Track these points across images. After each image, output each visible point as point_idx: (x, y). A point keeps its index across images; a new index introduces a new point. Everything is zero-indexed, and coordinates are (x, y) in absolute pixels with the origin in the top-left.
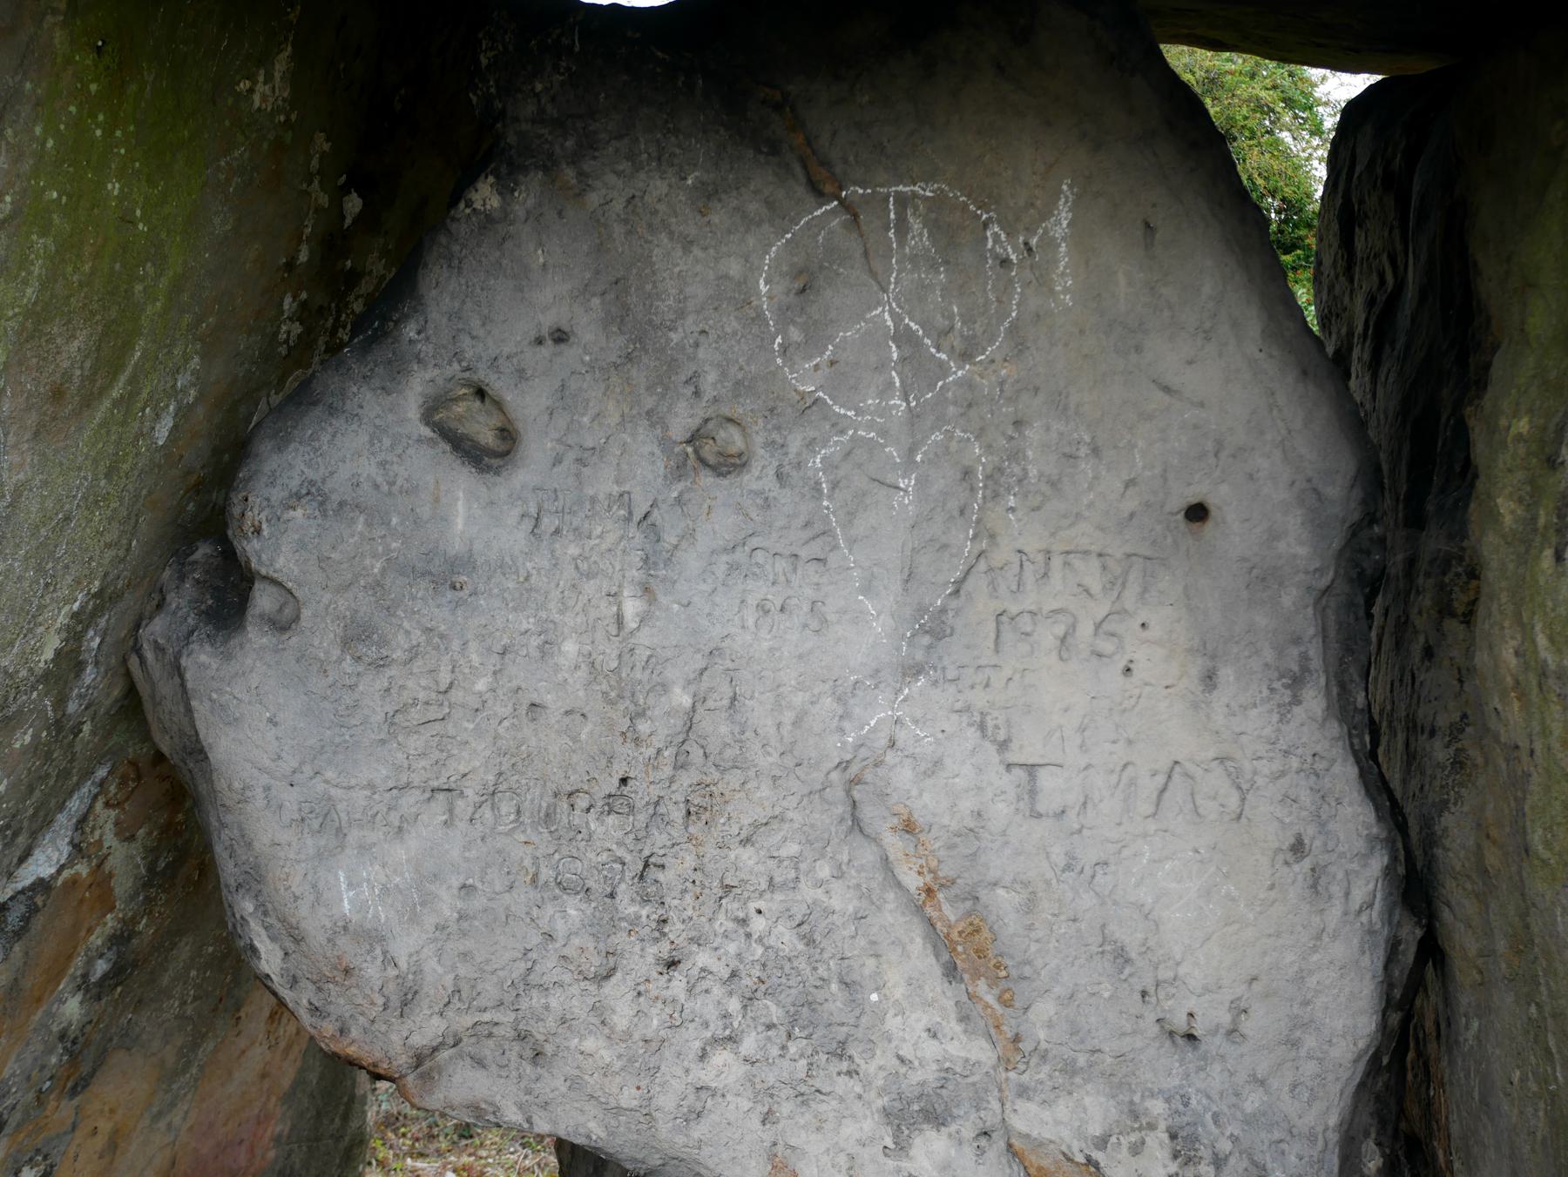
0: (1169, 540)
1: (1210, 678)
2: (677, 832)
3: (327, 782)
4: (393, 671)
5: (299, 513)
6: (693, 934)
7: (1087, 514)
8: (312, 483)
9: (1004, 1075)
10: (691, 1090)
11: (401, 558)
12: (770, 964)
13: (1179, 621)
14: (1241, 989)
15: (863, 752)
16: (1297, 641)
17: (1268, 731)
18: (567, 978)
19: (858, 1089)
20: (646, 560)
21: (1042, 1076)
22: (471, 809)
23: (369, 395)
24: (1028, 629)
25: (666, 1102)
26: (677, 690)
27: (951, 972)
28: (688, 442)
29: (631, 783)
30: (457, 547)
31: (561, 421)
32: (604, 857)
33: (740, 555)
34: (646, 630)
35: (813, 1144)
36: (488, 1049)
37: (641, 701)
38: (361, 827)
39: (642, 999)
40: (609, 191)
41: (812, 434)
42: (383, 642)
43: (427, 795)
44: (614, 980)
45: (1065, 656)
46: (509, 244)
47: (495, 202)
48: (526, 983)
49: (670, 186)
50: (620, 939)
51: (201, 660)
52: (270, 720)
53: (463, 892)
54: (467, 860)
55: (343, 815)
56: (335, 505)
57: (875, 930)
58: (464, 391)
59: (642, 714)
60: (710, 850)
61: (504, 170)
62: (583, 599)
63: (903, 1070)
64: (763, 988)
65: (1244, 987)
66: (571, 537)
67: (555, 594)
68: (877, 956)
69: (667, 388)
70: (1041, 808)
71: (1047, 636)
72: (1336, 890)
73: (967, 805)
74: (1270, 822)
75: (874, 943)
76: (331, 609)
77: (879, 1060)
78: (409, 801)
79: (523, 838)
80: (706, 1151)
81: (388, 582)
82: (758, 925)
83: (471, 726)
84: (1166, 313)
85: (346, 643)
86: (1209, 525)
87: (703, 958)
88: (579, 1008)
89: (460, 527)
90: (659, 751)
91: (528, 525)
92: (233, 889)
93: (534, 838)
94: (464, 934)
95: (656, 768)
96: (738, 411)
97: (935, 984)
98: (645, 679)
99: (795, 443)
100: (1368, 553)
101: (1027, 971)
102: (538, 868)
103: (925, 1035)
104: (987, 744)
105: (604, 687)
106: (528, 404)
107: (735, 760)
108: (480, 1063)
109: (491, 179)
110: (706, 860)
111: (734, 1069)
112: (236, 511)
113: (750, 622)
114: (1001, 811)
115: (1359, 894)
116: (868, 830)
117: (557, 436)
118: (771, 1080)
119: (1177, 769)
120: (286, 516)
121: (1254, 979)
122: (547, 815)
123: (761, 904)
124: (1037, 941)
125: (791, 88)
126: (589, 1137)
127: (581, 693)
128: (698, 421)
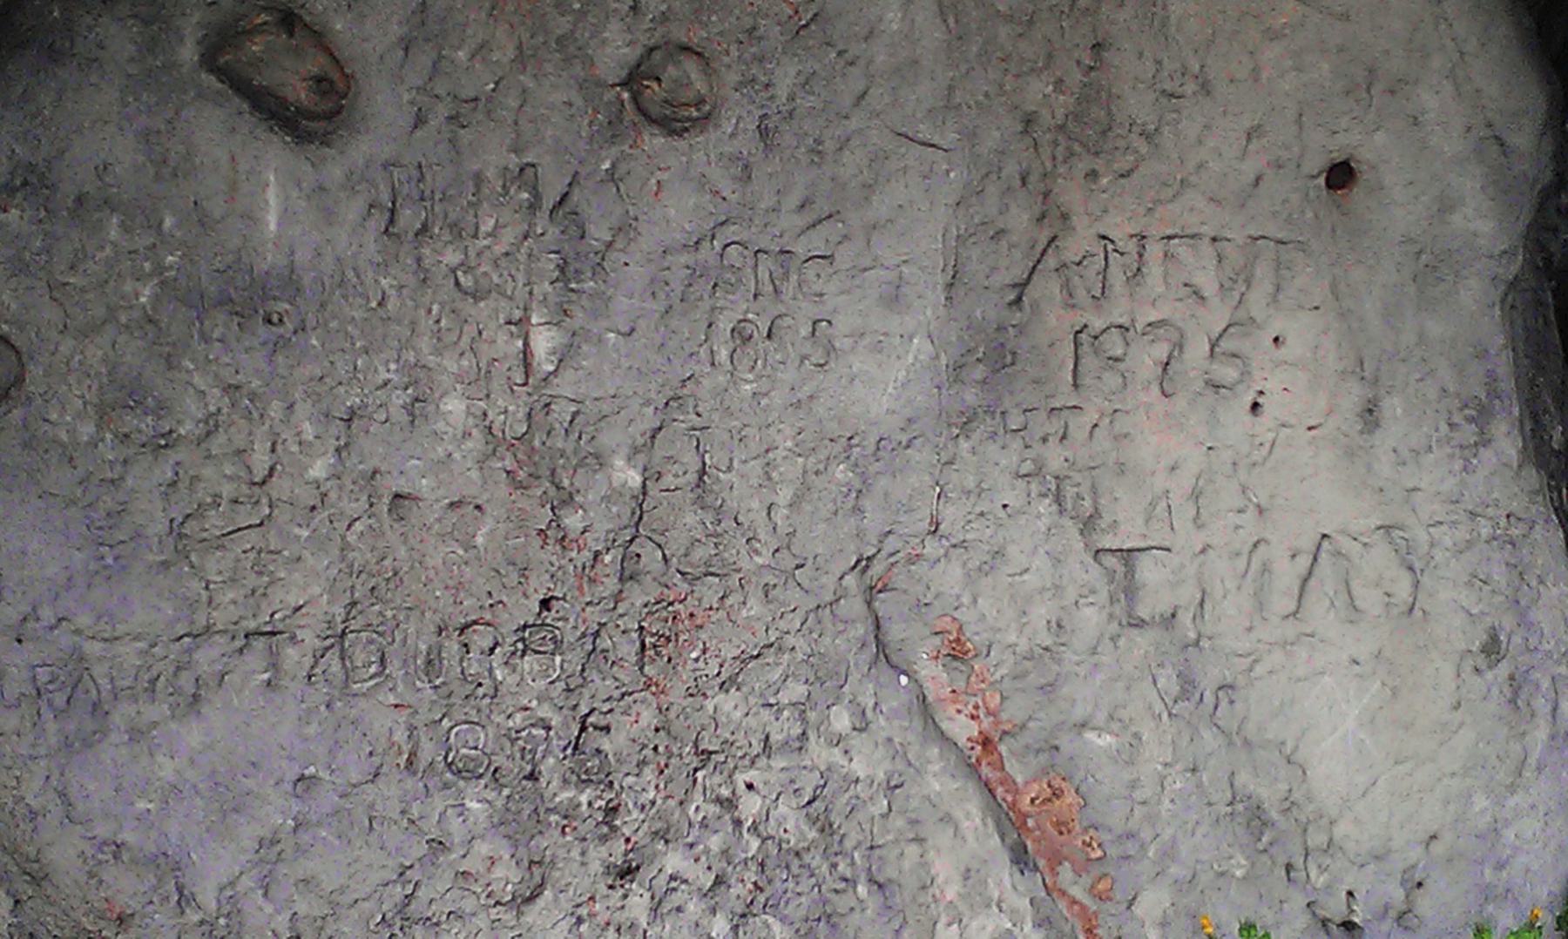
0: (1309, 215)
1: (1370, 411)
3: (78, 632)
4: (180, 454)
5: (14, 213)
6: (659, 825)
7: (1193, 179)
8: (31, 167)
11: (183, 282)
12: (770, 863)
14: (1416, 854)
16: (1482, 355)
17: (1450, 485)
18: (469, 905)
20: (562, 269)
22: (308, 661)
24: (1119, 352)
26: (619, 462)
27: (1020, 858)
28: (623, 84)
29: (555, 605)
30: (271, 259)
31: (423, 59)
33: (707, 253)
34: (568, 375)
37: (566, 483)
38: (135, 699)
39: (584, 928)
41: (811, 65)
42: (161, 410)
44: (540, 902)
50: (548, 842)
55: (104, 682)
56: (70, 203)
57: (914, 803)
59: (569, 500)
60: (676, 695)
62: (469, 330)
65: (1420, 850)
66: (447, 237)
67: (427, 324)
68: (919, 840)
70: (1143, 612)
71: (1146, 357)
72: (1542, 705)
73: (1041, 612)
75: (914, 822)
76: (75, 364)
78: (207, 658)
79: (392, 700)
82: (751, 807)
83: (305, 533)
85: (103, 416)
86: (1358, 193)
87: (674, 861)
89: (273, 227)
90: (597, 555)
91: (379, 220)
93: (409, 698)
95: (592, 581)
96: (696, 37)
97: (1002, 876)
98: (570, 447)
99: (784, 86)
101: (1131, 848)
102: (417, 744)
105: (509, 463)
107: (708, 564)
110: (672, 715)
113: (723, 355)
114: (1091, 619)
116: (894, 659)
119: (1326, 544)
121: (1434, 837)
122: (429, 662)
124: (1144, 803)
127: (474, 474)
128: (639, 51)
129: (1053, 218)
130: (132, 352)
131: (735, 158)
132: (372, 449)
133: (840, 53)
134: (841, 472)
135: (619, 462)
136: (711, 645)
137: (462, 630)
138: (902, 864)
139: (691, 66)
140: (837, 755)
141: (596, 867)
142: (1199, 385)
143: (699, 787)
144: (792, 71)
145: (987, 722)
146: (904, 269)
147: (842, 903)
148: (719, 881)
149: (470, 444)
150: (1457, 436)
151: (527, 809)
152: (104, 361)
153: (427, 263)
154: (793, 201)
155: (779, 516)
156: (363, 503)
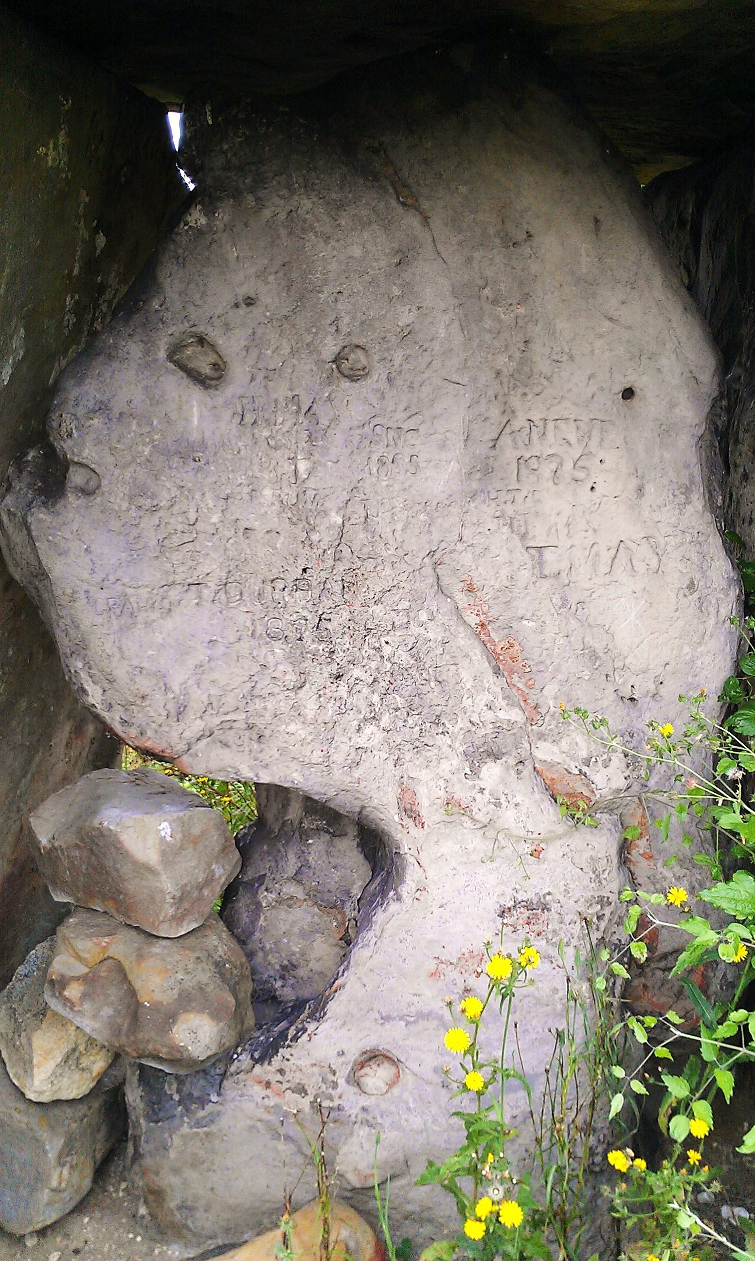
2: (337, 598)
3: (124, 585)
5: (96, 420)
8: (101, 402)
9: (530, 728)
10: (353, 749)
11: (161, 445)
13: (622, 457)
15: (443, 545)
17: (673, 520)
18: (276, 690)
19: (449, 742)
21: (552, 726)
22: (213, 595)
23: (133, 346)
24: (535, 467)
25: (338, 757)
26: (333, 514)
27: (497, 672)
28: (333, 362)
30: (195, 436)
31: (254, 353)
32: (295, 617)
33: (367, 429)
34: (312, 479)
35: (424, 775)
36: (230, 736)
37: (312, 522)
39: (321, 699)
40: (276, 207)
41: (408, 352)
42: (153, 496)
43: (186, 588)
44: (304, 689)
45: (556, 482)
46: (214, 246)
47: (203, 221)
48: (252, 695)
49: (313, 203)
51: (40, 517)
52: (86, 549)
53: (210, 644)
54: (212, 625)
57: (454, 649)
58: (192, 340)
60: (357, 607)
61: (207, 199)
62: (274, 462)
63: (474, 729)
64: (392, 687)
65: (662, 669)
66: (264, 425)
67: (256, 460)
69: (318, 329)
70: (546, 572)
71: (547, 469)
72: (712, 610)
73: (504, 572)
74: (676, 571)
77: (460, 725)
78: (174, 594)
80: (363, 784)
81: (154, 459)
82: (387, 650)
84: (609, 273)
85: (131, 498)
86: (635, 401)
87: (357, 672)
88: (284, 707)
89: (196, 423)
91: (237, 419)
92: (69, 656)
94: (212, 669)
96: (362, 341)
97: (489, 678)
98: (314, 507)
99: (398, 360)
100: (720, 416)
103: (485, 708)
104: (514, 535)
105: (290, 515)
106: (231, 345)
108: (227, 745)
109: (199, 207)
110: (355, 614)
111: (377, 735)
112: (55, 424)
114: (525, 575)
115: (724, 611)
116: (445, 592)
117: (252, 363)
118: (399, 741)
120: (88, 424)
122: (259, 594)
123: (387, 639)
125: (383, 139)
126: (293, 782)
127: (276, 520)
128: (339, 348)
129: (509, 412)
130: (142, 474)
131: (377, 391)
132: (236, 510)
133: (421, 347)
134: (422, 517)
135: (333, 514)
136: (371, 586)
137: (272, 581)
138: (448, 675)
139: (360, 352)
140: (422, 630)
141: (326, 675)
142: (569, 480)
143: (367, 643)
144: (401, 354)
145: (483, 617)
146: (447, 434)
147: (425, 689)
148: (375, 680)
149: (274, 508)
150: (677, 500)
151: (299, 652)
152: (131, 477)
153: (256, 436)
154: (402, 407)
155: (397, 534)
156: (233, 532)
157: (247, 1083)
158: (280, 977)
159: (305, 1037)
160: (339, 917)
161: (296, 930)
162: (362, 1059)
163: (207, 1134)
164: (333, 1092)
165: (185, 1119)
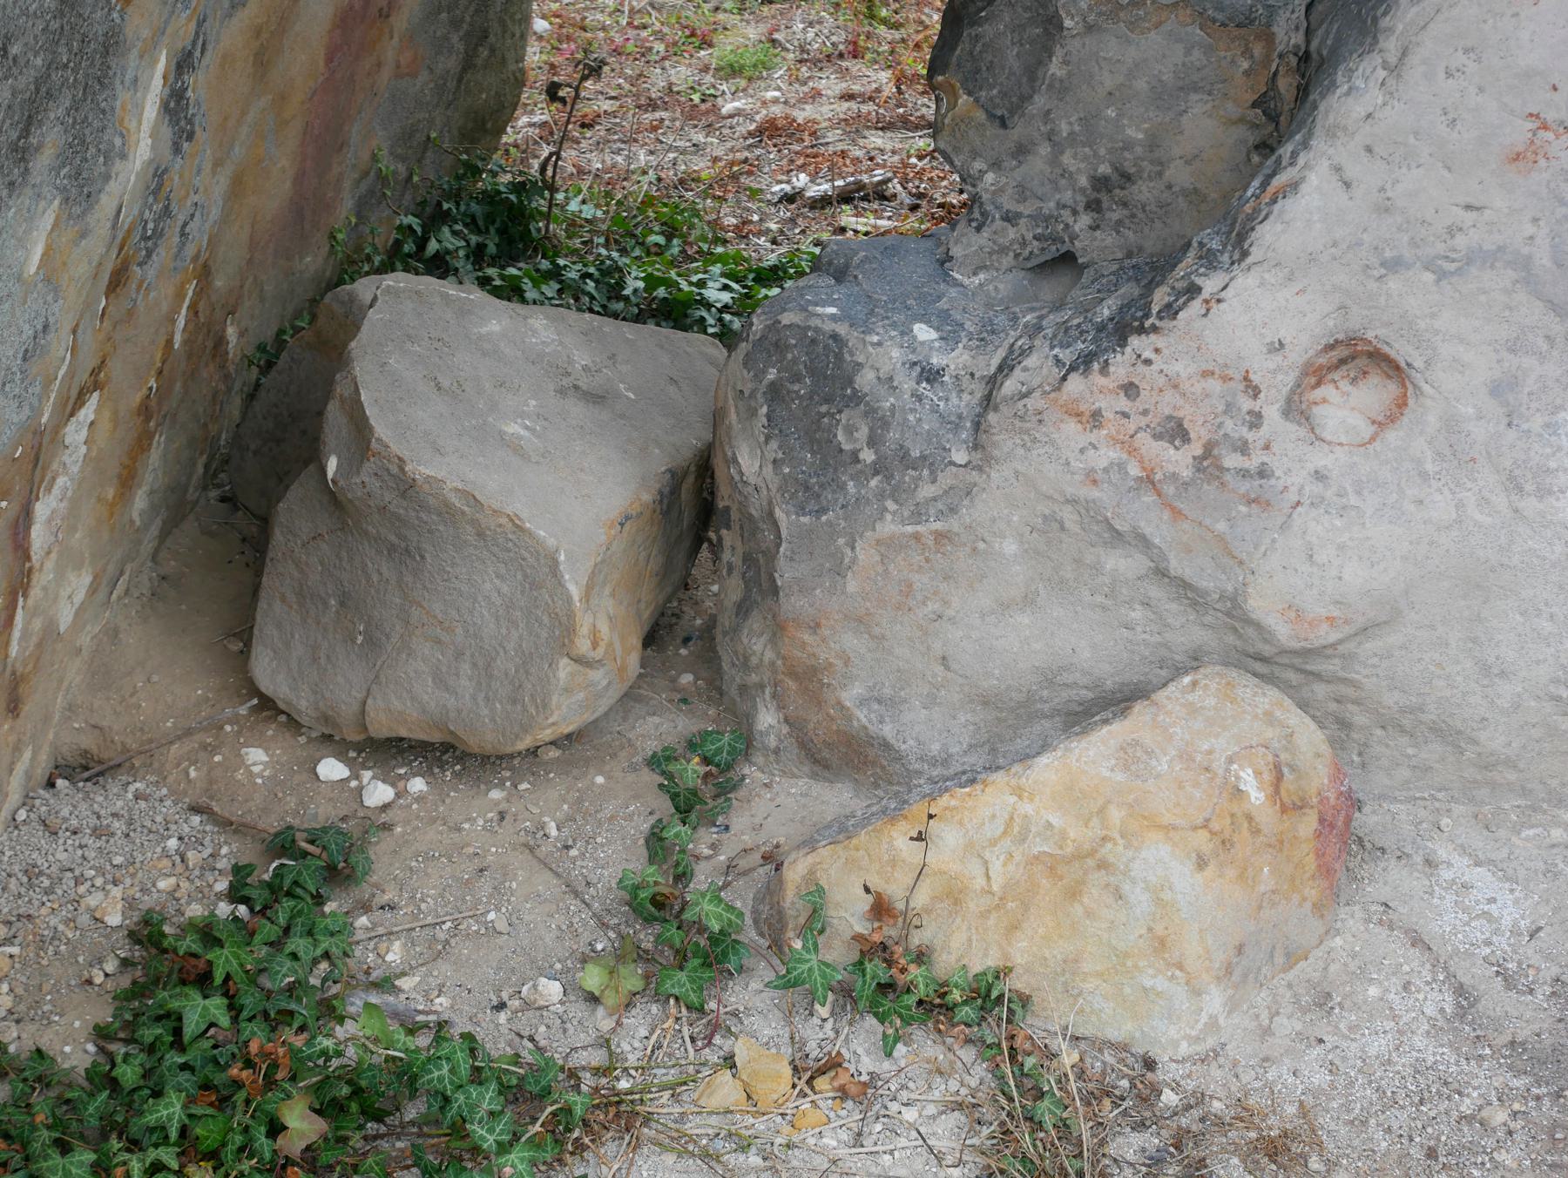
157: (1045, 416)
158: (1088, 207)
159: (1196, 306)
160: (1258, 50)
161: (1141, 84)
162: (1323, 360)
163: (940, 536)
164: (1250, 436)
165: (891, 505)
